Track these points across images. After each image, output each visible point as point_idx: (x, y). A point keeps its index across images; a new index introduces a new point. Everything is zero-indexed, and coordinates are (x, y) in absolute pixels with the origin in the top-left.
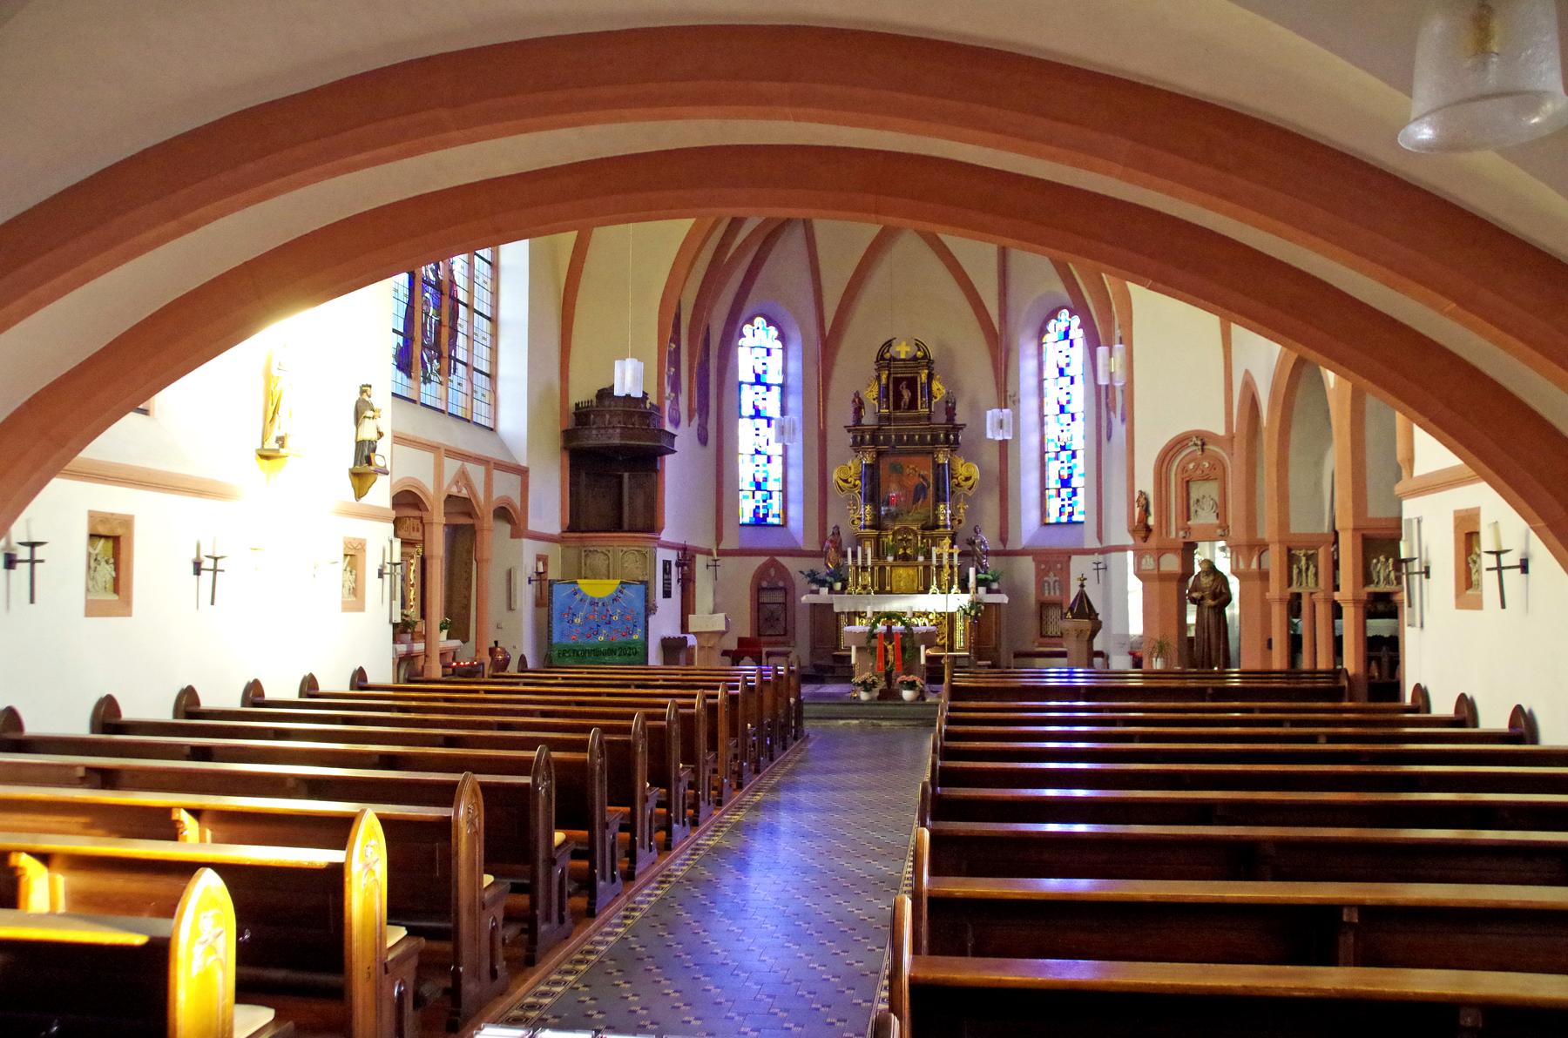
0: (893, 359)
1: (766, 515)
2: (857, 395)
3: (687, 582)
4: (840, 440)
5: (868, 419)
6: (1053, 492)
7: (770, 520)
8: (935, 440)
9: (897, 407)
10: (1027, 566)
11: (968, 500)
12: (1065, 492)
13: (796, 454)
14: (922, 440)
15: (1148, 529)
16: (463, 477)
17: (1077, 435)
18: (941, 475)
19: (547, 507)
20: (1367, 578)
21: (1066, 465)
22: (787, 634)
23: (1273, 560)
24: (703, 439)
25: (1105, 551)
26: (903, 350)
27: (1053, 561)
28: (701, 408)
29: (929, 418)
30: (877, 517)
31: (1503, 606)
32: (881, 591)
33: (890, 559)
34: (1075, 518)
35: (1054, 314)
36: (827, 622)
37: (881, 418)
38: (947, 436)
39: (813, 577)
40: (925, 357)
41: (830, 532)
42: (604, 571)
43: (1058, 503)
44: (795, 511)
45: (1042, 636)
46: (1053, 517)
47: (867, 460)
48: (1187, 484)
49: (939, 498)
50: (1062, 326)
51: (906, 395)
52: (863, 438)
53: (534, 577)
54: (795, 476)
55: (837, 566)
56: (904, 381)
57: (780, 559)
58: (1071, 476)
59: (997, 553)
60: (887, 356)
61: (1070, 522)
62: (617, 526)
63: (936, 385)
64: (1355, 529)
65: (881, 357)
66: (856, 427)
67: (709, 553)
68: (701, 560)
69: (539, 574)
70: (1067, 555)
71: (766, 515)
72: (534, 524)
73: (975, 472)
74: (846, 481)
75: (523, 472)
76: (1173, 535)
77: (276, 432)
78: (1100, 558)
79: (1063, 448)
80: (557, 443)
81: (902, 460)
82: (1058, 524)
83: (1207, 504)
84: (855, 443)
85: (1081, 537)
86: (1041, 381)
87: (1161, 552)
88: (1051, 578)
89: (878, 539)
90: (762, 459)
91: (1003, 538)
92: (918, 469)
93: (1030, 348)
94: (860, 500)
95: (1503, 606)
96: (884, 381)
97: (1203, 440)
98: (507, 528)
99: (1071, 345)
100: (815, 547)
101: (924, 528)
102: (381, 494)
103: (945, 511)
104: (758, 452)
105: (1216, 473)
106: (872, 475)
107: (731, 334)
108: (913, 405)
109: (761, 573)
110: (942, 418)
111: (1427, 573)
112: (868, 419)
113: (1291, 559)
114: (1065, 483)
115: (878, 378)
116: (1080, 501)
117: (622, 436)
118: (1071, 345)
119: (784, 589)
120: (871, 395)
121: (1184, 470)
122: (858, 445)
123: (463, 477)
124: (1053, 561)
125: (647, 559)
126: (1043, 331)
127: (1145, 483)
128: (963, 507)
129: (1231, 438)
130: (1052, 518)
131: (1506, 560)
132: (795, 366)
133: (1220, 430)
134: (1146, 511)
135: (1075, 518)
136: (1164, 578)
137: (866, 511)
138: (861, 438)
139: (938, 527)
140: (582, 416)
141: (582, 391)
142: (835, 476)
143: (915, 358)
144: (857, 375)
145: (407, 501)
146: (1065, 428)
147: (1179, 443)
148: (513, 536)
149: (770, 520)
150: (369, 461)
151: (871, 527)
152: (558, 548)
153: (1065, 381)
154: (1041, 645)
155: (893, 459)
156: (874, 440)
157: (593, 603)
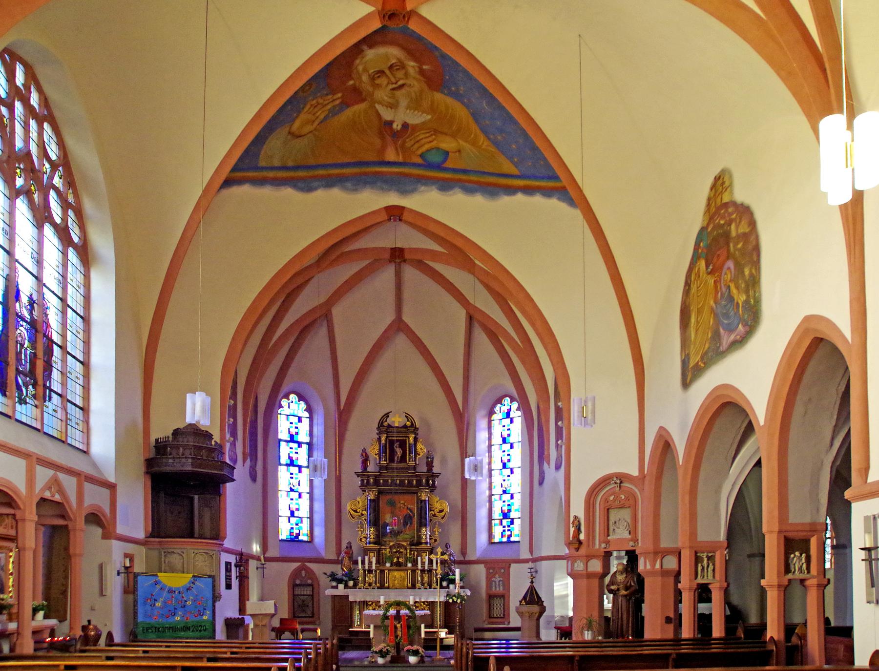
0: (389, 426)
1: (298, 534)
2: (364, 451)
4: (351, 483)
5: (372, 468)
6: (497, 522)
7: (301, 538)
8: (419, 483)
9: (392, 460)
10: (480, 571)
11: (440, 525)
12: (505, 522)
13: (319, 492)
14: (410, 484)
17: (516, 483)
18: (422, 507)
21: (506, 503)
22: (314, 617)
24: (254, 478)
26: (397, 420)
28: (251, 454)
29: (415, 468)
30: (378, 536)
32: (382, 587)
33: (388, 565)
34: (512, 539)
36: (343, 610)
37: (381, 467)
38: (427, 481)
39: (333, 577)
40: (412, 425)
41: (344, 545)
42: (179, 567)
43: (501, 529)
44: (319, 532)
45: (490, 617)
46: (497, 538)
47: (371, 496)
49: (422, 524)
50: (505, 409)
51: (399, 452)
52: (368, 481)
53: (123, 570)
54: (319, 507)
55: (350, 570)
56: (397, 442)
57: (308, 564)
58: (509, 511)
59: (460, 563)
60: (386, 424)
61: (509, 542)
62: (190, 534)
63: (419, 446)
65: (381, 424)
66: (363, 473)
67: (258, 559)
68: (253, 564)
69: (126, 568)
70: (507, 563)
71: (298, 534)
72: (120, 529)
73: (446, 507)
74: (356, 511)
78: (530, 565)
79: (504, 492)
81: (396, 498)
82: (501, 543)
84: (362, 485)
85: (518, 551)
86: (490, 446)
89: (379, 551)
90: (295, 495)
91: (464, 552)
92: (407, 504)
93: (483, 424)
94: (366, 524)
96: (383, 442)
98: (99, 531)
99: (512, 422)
100: (333, 557)
101: (412, 544)
103: (426, 533)
104: (292, 490)
106: (374, 507)
107: (273, 405)
108: (403, 459)
110: (425, 469)
112: (372, 468)
114: (505, 515)
115: (379, 439)
116: (516, 528)
118: (512, 422)
119: (311, 585)
120: (373, 451)
122: (364, 486)
124: (498, 568)
126: (491, 412)
128: (437, 531)
130: (497, 538)
132: (318, 430)
135: (512, 539)
138: (366, 481)
139: (421, 543)
142: (348, 508)
143: (405, 426)
144: (363, 437)
146: (506, 478)
148: (106, 536)
149: (301, 538)
151: (375, 543)
152: (143, 549)
153: (506, 447)
154: (490, 623)
155: (389, 497)
156: (376, 483)
157: (171, 591)
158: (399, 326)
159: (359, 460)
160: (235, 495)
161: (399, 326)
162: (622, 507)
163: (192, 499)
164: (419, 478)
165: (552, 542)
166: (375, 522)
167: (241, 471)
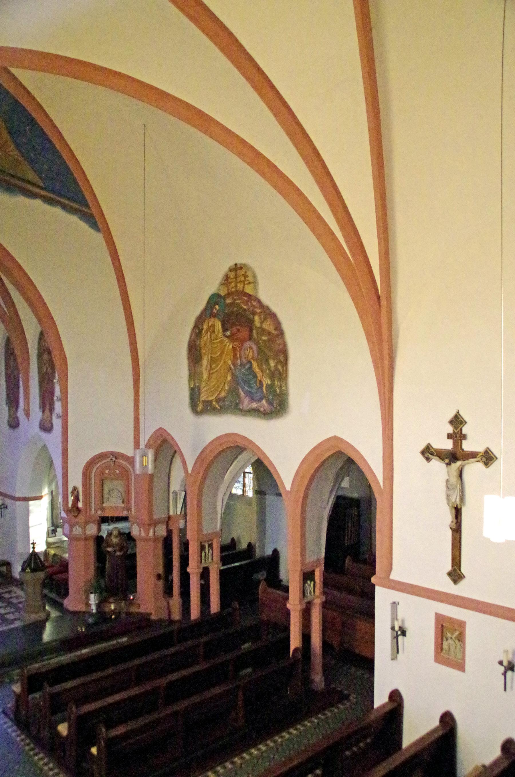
15: (79, 510)
31: (505, 690)
76: (93, 512)
83: (115, 494)
87: (87, 523)
95: (505, 690)
97: (116, 456)
113: (202, 548)
127: (76, 480)
134: (77, 499)
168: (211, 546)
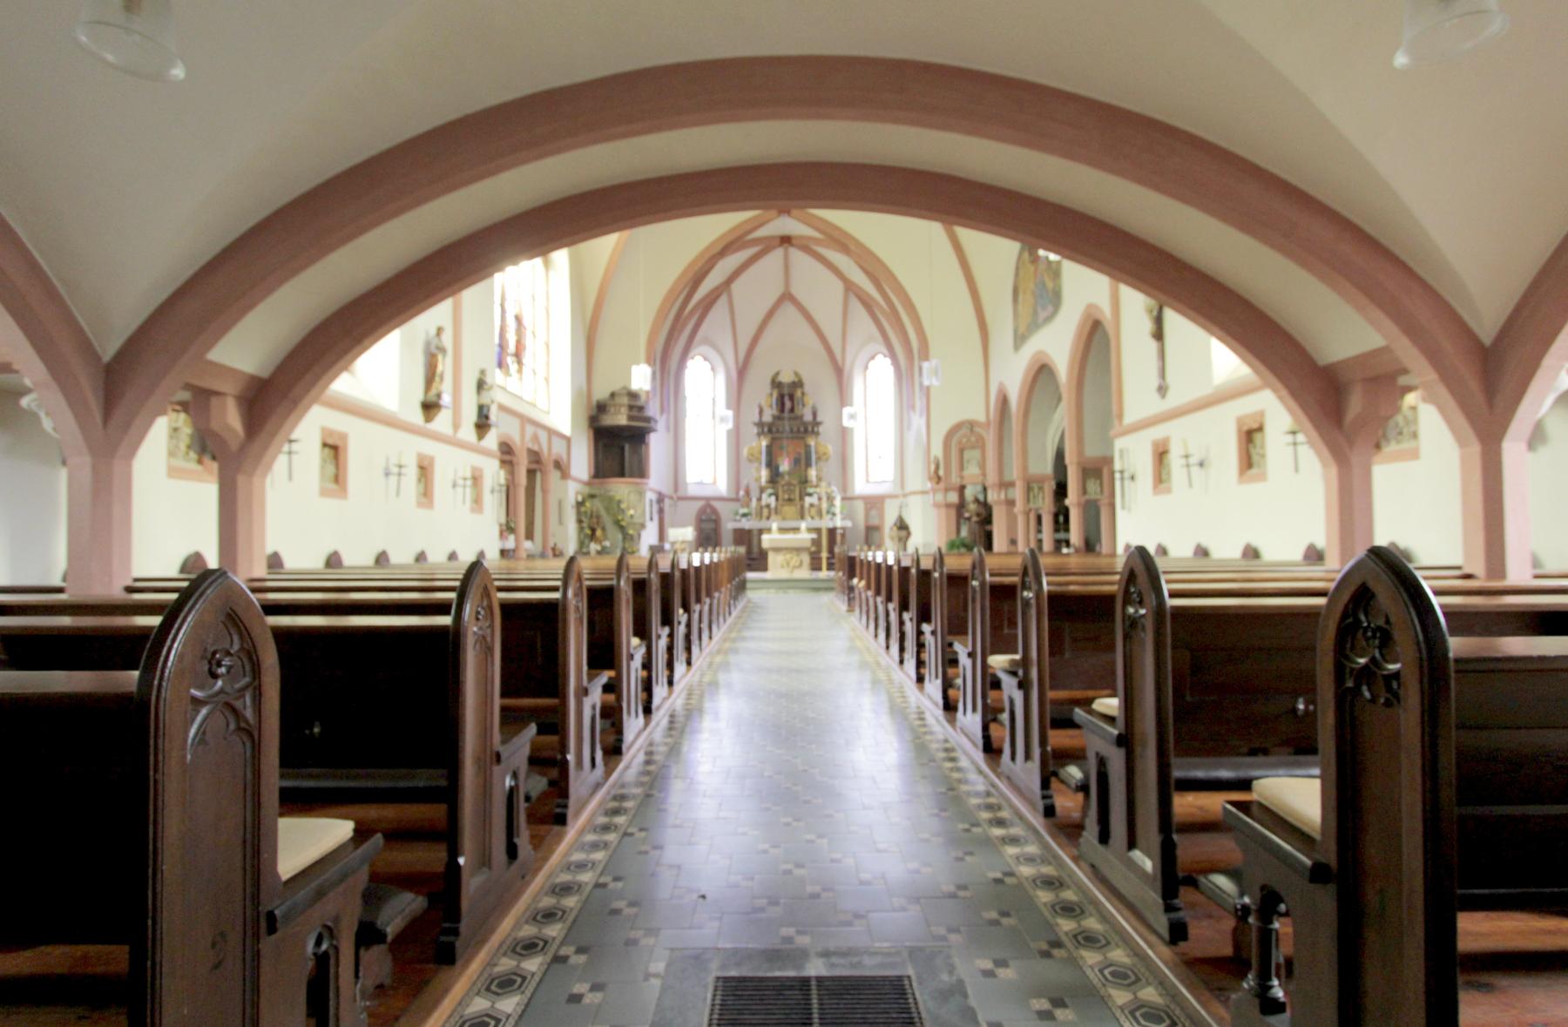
3: (661, 511)
5: (767, 418)
9: (782, 409)
10: (860, 507)
15: (939, 479)
16: (535, 438)
19: (581, 461)
20: (1084, 491)
23: (1018, 493)
24: (668, 429)
25: (905, 496)
26: (786, 378)
27: (874, 503)
35: (873, 358)
48: (961, 451)
51: (788, 404)
56: (787, 395)
64: (1079, 464)
66: (760, 424)
68: (667, 502)
75: (568, 440)
77: (433, 392)
80: (584, 423)
87: (947, 490)
88: (874, 513)
97: (972, 424)
102: (491, 441)
105: (980, 444)
108: (792, 410)
109: (702, 511)
111: (1132, 478)
113: (1029, 489)
117: (630, 418)
121: (960, 442)
123: (535, 438)
125: (641, 494)
126: (866, 368)
127: (937, 451)
129: (988, 423)
131: (1193, 460)
133: (981, 418)
136: (948, 506)
137: (764, 474)
140: (601, 408)
141: (601, 393)
145: (506, 450)
147: (957, 428)
150: (487, 417)
156: (770, 431)
158: (787, 297)
159: (757, 411)
160: (657, 445)
161: (787, 297)
162: (973, 447)
163: (622, 449)
164: (805, 425)
165: (918, 479)
166: (772, 464)
167: (661, 425)
168: (1041, 488)
